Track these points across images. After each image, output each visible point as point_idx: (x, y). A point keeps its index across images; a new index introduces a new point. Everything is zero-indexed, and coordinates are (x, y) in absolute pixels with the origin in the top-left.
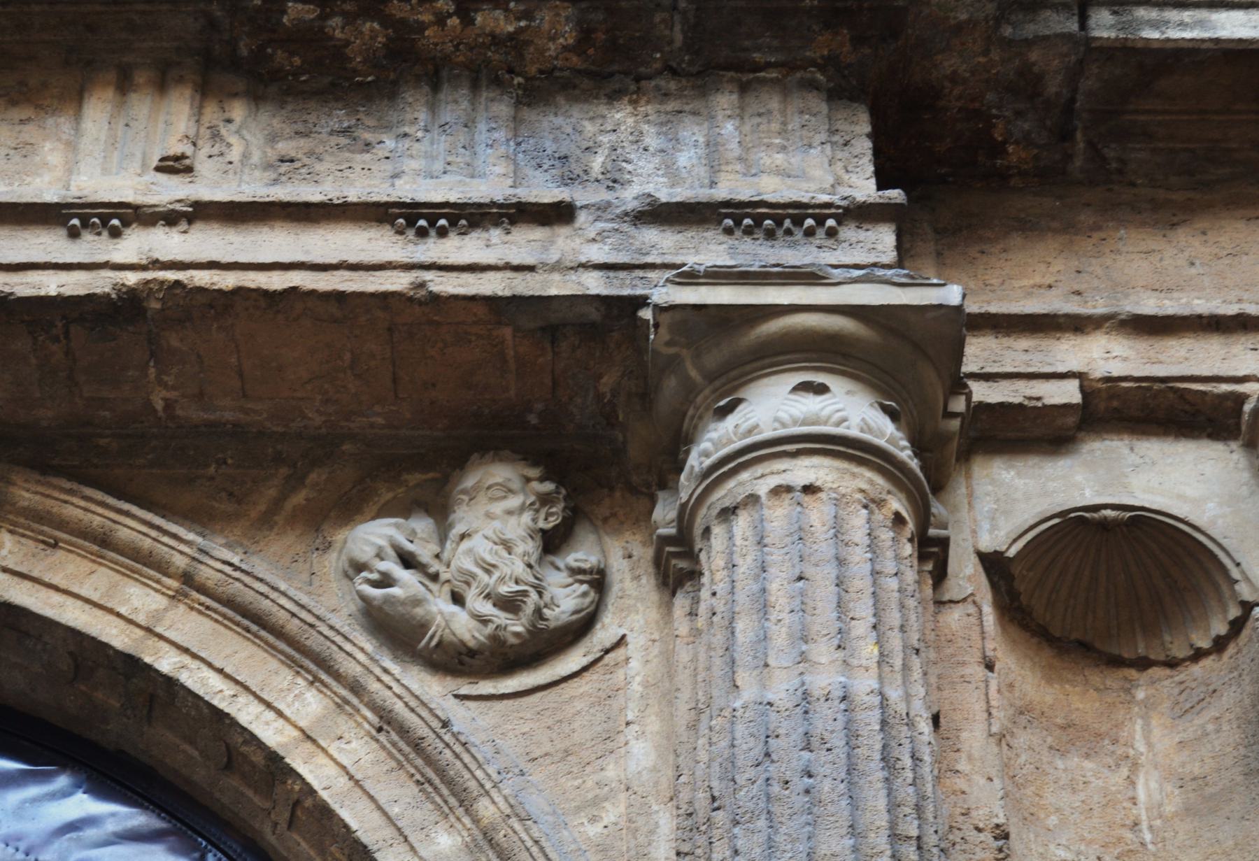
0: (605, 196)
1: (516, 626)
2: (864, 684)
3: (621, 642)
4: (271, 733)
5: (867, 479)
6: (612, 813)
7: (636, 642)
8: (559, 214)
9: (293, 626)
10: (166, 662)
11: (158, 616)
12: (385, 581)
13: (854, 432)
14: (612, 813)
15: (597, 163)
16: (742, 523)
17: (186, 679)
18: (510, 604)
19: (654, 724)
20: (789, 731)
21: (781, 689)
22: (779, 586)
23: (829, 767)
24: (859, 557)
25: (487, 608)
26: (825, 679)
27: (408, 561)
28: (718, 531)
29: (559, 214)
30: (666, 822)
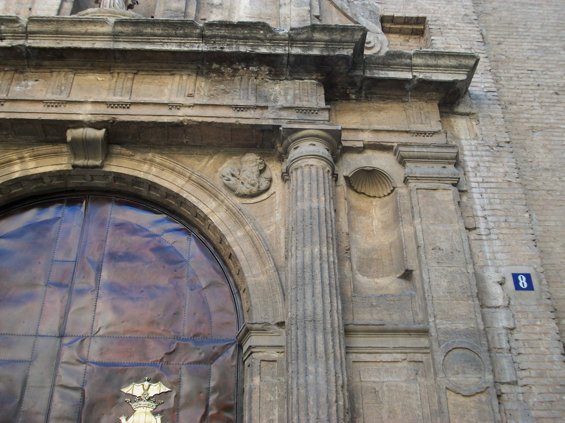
0: (274, 104)
1: (254, 190)
2: (322, 206)
3: (274, 193)
4: (206, 210)
5: (323, 163)
6: (272, 228)
7: (277, 193)
8: (266, 108)
9: (210, 189)
10: (185, 195)
11: (183, 185)
12: (229, 180)
13: (321, 154)
14: (272, 228)
15: (272, 98)
16: (299, 171)
17: (188, 199)
18: (253, 185)
19: (281, 210)
20: (308, 216)
21: (306, 206)
22: (306, 186)
23: (316, 222)
24: (321, 180)
25: (249, 186)
26: (315, 205)
27: (233, 175)
28: (294, 172)
29: (266, 108)
30: (283, 231)
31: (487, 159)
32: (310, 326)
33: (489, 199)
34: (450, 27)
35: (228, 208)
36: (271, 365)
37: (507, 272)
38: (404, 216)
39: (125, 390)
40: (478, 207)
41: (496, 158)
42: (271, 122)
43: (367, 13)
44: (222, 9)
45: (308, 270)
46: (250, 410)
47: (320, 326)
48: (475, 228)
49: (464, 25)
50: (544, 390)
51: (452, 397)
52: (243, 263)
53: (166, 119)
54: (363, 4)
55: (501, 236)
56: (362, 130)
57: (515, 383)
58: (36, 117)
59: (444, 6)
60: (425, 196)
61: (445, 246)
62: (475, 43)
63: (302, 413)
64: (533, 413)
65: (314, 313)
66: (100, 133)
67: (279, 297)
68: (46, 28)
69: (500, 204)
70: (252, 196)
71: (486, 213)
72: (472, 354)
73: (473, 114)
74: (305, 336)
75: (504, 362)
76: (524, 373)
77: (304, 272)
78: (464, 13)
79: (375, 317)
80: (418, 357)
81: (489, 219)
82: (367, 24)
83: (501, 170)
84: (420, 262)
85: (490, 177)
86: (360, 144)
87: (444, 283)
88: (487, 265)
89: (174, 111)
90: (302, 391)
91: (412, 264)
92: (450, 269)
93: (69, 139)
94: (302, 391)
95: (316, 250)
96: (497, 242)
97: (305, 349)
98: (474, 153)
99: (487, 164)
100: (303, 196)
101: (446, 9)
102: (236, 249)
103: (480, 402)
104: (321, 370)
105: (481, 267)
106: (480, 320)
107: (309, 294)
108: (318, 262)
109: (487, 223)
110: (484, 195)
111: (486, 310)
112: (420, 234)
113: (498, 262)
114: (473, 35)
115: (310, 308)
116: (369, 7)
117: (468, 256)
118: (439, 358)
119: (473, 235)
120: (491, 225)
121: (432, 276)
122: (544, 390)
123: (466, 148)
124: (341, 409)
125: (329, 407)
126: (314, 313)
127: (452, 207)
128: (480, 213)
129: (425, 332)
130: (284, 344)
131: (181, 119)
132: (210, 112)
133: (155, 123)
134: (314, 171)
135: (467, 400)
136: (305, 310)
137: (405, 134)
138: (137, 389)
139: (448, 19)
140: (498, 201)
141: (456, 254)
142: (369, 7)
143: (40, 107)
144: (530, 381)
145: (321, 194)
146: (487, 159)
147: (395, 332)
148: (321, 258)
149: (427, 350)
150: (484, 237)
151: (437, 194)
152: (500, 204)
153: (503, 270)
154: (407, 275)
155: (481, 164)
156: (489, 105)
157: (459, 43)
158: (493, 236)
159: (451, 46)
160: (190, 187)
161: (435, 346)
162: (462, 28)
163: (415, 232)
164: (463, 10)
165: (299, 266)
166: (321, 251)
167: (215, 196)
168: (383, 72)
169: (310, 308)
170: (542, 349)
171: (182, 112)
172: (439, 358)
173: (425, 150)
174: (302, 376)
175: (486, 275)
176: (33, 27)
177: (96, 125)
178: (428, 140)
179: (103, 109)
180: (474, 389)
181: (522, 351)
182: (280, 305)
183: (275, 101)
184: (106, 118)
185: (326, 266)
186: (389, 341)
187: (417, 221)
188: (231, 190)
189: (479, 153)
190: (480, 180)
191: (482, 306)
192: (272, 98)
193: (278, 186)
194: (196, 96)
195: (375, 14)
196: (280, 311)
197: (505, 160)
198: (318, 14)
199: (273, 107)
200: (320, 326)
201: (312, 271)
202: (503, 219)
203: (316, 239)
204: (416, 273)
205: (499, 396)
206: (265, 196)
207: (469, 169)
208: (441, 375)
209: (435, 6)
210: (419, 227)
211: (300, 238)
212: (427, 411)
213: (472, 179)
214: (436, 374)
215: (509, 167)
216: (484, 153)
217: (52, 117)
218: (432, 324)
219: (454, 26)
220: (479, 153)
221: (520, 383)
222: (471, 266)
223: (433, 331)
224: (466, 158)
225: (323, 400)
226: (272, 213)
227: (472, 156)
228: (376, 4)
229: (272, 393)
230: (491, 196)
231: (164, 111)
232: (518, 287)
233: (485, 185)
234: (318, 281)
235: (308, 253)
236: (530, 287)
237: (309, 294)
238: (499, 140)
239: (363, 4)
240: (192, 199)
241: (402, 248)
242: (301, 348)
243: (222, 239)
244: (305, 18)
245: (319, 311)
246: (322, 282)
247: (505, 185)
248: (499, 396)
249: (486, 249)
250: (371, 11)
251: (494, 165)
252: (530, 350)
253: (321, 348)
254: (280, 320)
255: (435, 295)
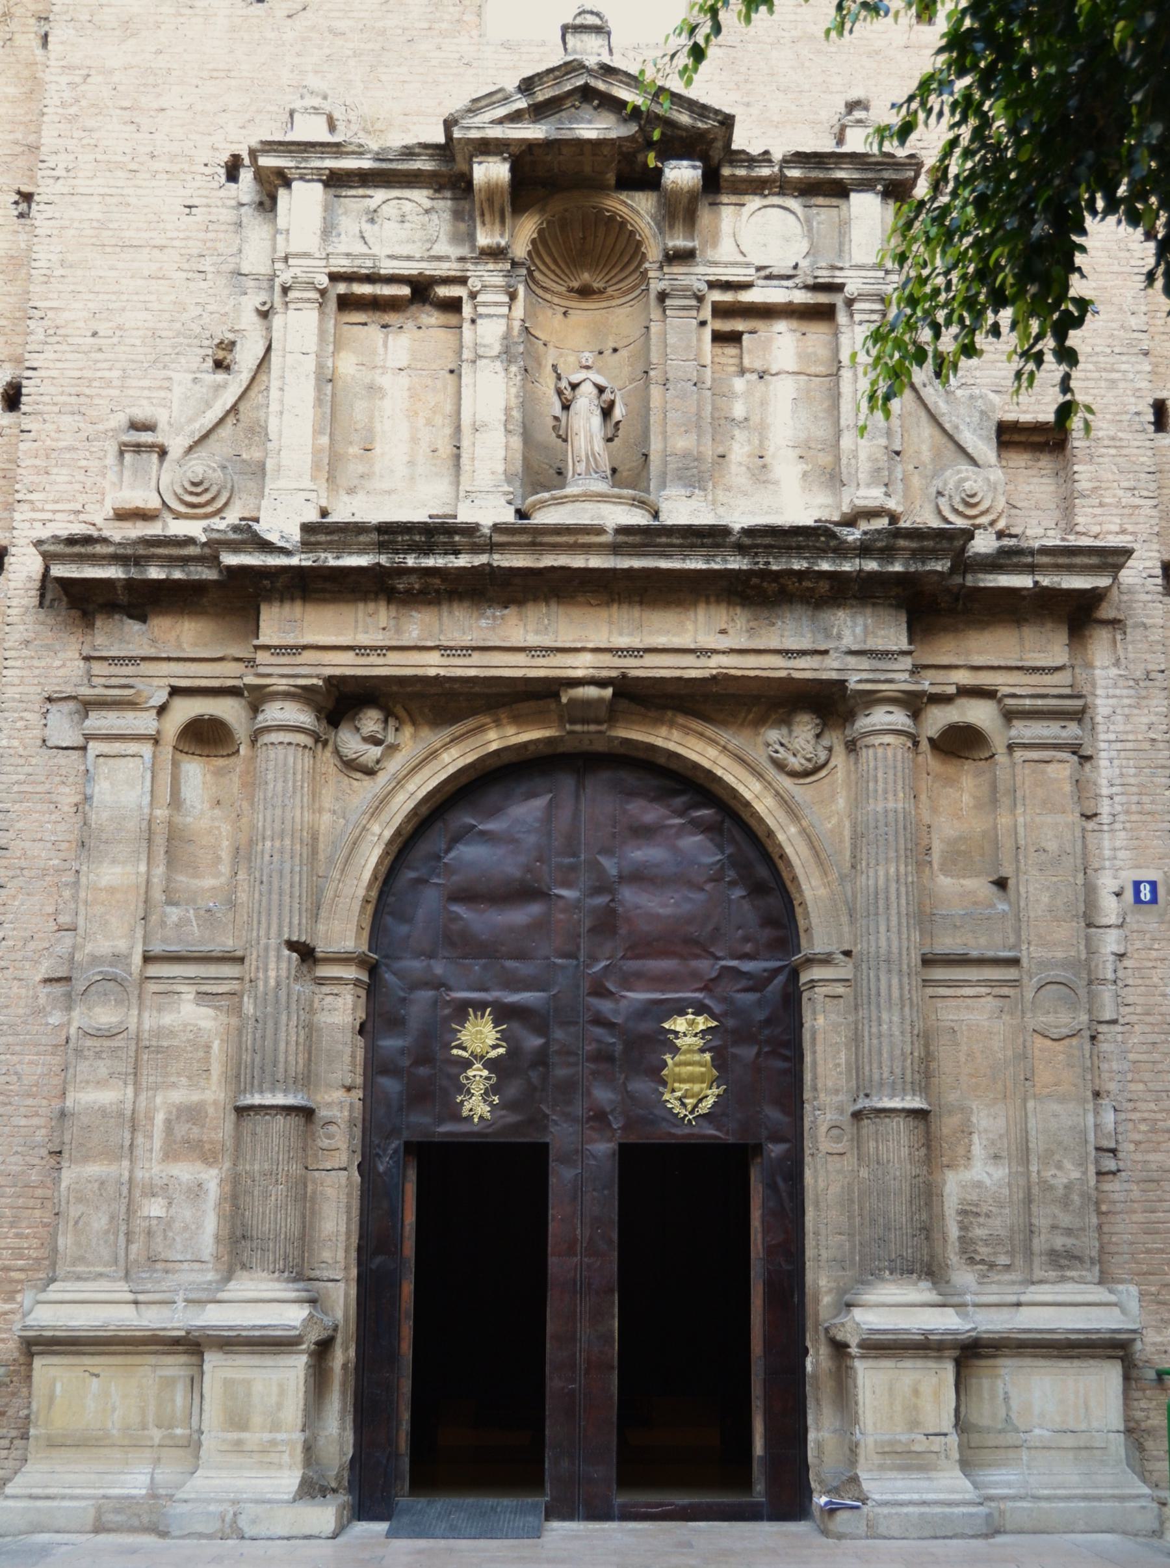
1: (810, 766)
2: (900, 805)
4: (748, 796)
10: (719, 772)
12: (777, 752)
14: (834, 820)
16: (871, 751)
18: (809, 760)
19: (844, 793)
21: (880, 808)
22: (880, 775)
23: (891, 830)
24: (899, 764)
30: (847, 824)
31: (1127, 701)
32: (883, 966)
33: (1121, 767)
34: (1106, 443)
35: (777, 794)
36: (835, 1001)
37: (1128, 876)
38: (1004, 799)
39: (666, 1025)
40: (1104, 782)
41: (1140, 701)
42: (834, 676)
43: (976, 418)
44: (747, 428)
45: (882, 896)
46: (814, 1052)
47: (895, 967)
48: (1096, 815)
49: (1129, 436)
50: (1148, 1029)
51: (1039, 1041)
52: (799, 871)
53: (693, 674)
54: (971, 397)
55: (1128, 825)
56: (957, 667)
57: (1114, 1022)
58: (518, 673)
59: (1103, 392)
60: (1034, 772)
61: (1052, 846)
62: (1143, 476)
63: (875, 1065)
64: (1131, 1056)
65: (889, 952)
66: (608, 692)
67: (845, 919)
68: (517, 539)
69: (1135, 775)
70: (806, 774)
71: (1114, 790)
72: (1067, 990)
73: (1120, 621)
74: (878, 980)
75: (1107, 994)
76: (1128, 1009)
77: (876, 898)
78: (1134, 409)
79: (958, 941)
80: (1005, 991)
81: (1117, 799)
82: (975, 447)
83: (1145, 720)
84: (1018, 869)
85: (1127, 732)
86: (952, 690)
87: (1045, 898)
88: (1104, 868)
89: (703, 661)
90: (875, 1041)
91: (1007, 871)
92: (1055, 879)
93: (564, 700)
94: (875, 1041)
95: (892, 870)
96: (1122, 834)
97: (879, 994)
98: (1111, 692)
99: (1127, 711)
100: (876, 791)
101: (1105, 401)
102: (789, 851)
103: (1071, 1047)
104: (896, 1019)
105: (1096, 870)
106: (1082, 947)
107: (883, 929)
108: (893, 887)
109: (1112, 806)
110: (1116, 762)
111: (1093, 930)
112: (1021, 830)
113: (1118, 863)
114: (1142, 459)
115: (883, 943)
116: (979, 403)
117: (1079, 861)
118: (1029, 995)
119: (1090, 825)
120: (1118, 808)
121: (1031, 889)
122: (1148, 1029)
123: (1100, 682)
124: (916, 1060)
125: (904, 1060)
126: (889, 952)
127: (1068, 788)
128: (1105, 791)
129: (1015, 962)
130: (850, 977)
131: (714, 672)
132: (751, 661)
133: (680, 679)
134: (890, 752)
135: (1056, 1044)
136: (878, 947)
137: (1016, 673)
138: (679, 1024)
139: (1105, 426)
140: (1132, 771)
141: (1064, 858)
142: (979, 403)
143: (520, 659)
144: (1133, 1019)
145: (899, 788)
146: (1127, 701)
147: (981, 962)
148: (898, 881)
149: (1015, 983)
150: (1106, 828)
151: (1050, 769)
152: (1135, 775)
153: (1123, 874)
154: (1001, 884)
155: (1119, 711)
156: (1145, 603)
157: (1117, 477)
158: (1118, 826)
159: (1103, 485)
160: (724, 761)
161: (1025, 980)
162: (1124, 444)
163: (1015, 826)
164: (1133, 400)
165: (872, 889)
166: (897, 870)
167: (759, 775)
168: (991, 577)
169: (883, 943)
170: (1155, 980)
171: (716, 661)
172: (1029, 995)
173: (1039, 702)
174: (874, 1024)
175: (1100, 882)
176: (497, 538)
177: (601, 683)
178: (1048, 679)
179: (607, 659)
180: (1065, 1031)
181: (1130, 982)
182: (846, 929)
183: (839, 637)
184: (614, 674)
185: (903, 890)
186: (972, 973)
187: (1020, 810)
188: (780, 766)
189: (1118, 692)
190: (1112, 737)
191: (1089, 925)
192: (835, 631)
193: (839, 759)
194: (731, 631)
195: (989, 417)
196: (847, 936)
197: (1155, 702)
198: (898, 449)
199: (837, 649)
200: (895, 967)
201: (887, 899)
202: (1135, 799)
203: (892, 854)
204: (1011, 883)
205: (1093, 1038)
206: (823, 773)
207: (1099, 719)
208: (1029, 1015)
209: (1087, 394)
210: (1021, 820)
211: (873, 851)
212: (1009, 1053)
213: (1102, 737)
214: (1023, 1012)
215: (1157, 714)
216: (1125, 692)
217: (541, 673)
218: (1024, 953)
219: (1113, 439)
220: (1118, 692)
221: (1121, 1021)
222: (1081, 875)
223: (1025, 962)
224: (1099, 701)
225: (898, 1052)
226: (833, 797)
227: (1108, 697)
228: (992, 396)
229: (839, 1033)
230: (1124, 762)
231: (689, 660)
232: (1138, 900)
233: (1119, 746)
234: (894, 911)
235: (881, 873)
236: (1154, 900)
237: (883, 929)
238: (1151, 667)
239: (971, 397)
240: (729, 779)
241: (996, 845)
242: (873, 992)
243: (770, 834)
244: (881, 464)
245: (895, 950)
246: (899, 913)
247: (1147, 746)
248: (1093, 1038)
249: (1106, 844)
250: (982, 413)
251: (1136, 711)
252: (1140, 982)
253: (896, 993)
254: (846, 947)
255: (1032, 915)
